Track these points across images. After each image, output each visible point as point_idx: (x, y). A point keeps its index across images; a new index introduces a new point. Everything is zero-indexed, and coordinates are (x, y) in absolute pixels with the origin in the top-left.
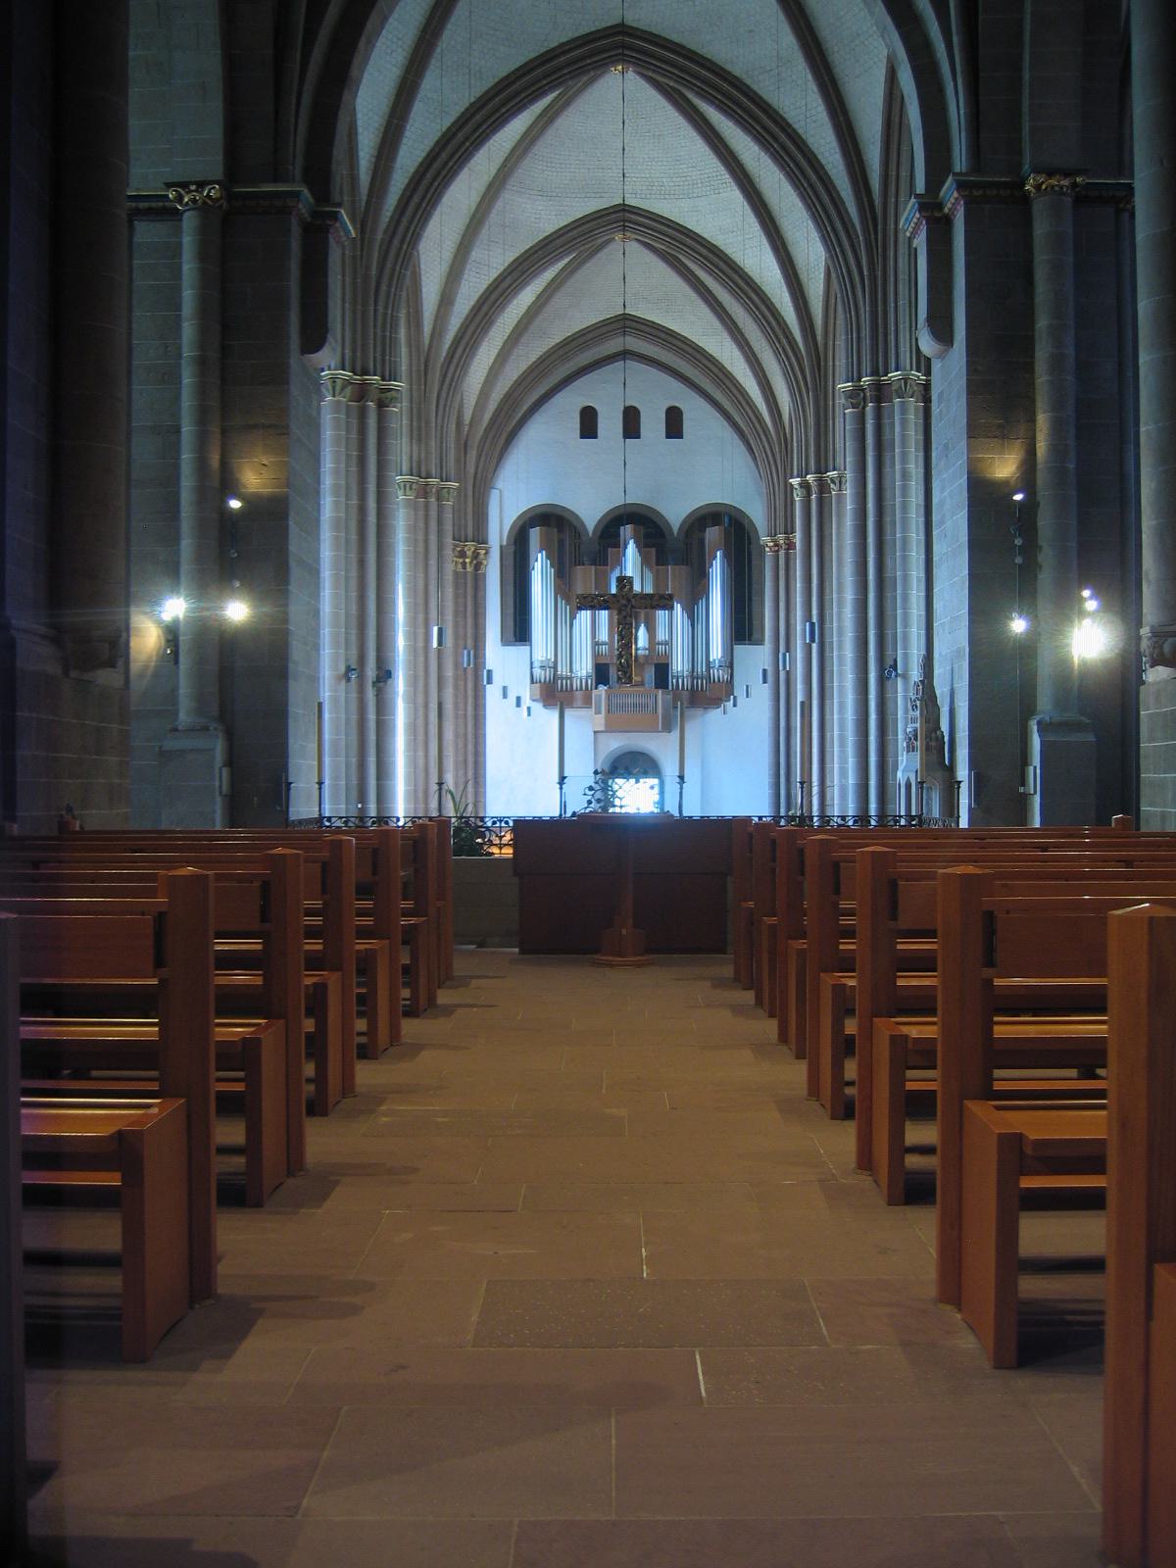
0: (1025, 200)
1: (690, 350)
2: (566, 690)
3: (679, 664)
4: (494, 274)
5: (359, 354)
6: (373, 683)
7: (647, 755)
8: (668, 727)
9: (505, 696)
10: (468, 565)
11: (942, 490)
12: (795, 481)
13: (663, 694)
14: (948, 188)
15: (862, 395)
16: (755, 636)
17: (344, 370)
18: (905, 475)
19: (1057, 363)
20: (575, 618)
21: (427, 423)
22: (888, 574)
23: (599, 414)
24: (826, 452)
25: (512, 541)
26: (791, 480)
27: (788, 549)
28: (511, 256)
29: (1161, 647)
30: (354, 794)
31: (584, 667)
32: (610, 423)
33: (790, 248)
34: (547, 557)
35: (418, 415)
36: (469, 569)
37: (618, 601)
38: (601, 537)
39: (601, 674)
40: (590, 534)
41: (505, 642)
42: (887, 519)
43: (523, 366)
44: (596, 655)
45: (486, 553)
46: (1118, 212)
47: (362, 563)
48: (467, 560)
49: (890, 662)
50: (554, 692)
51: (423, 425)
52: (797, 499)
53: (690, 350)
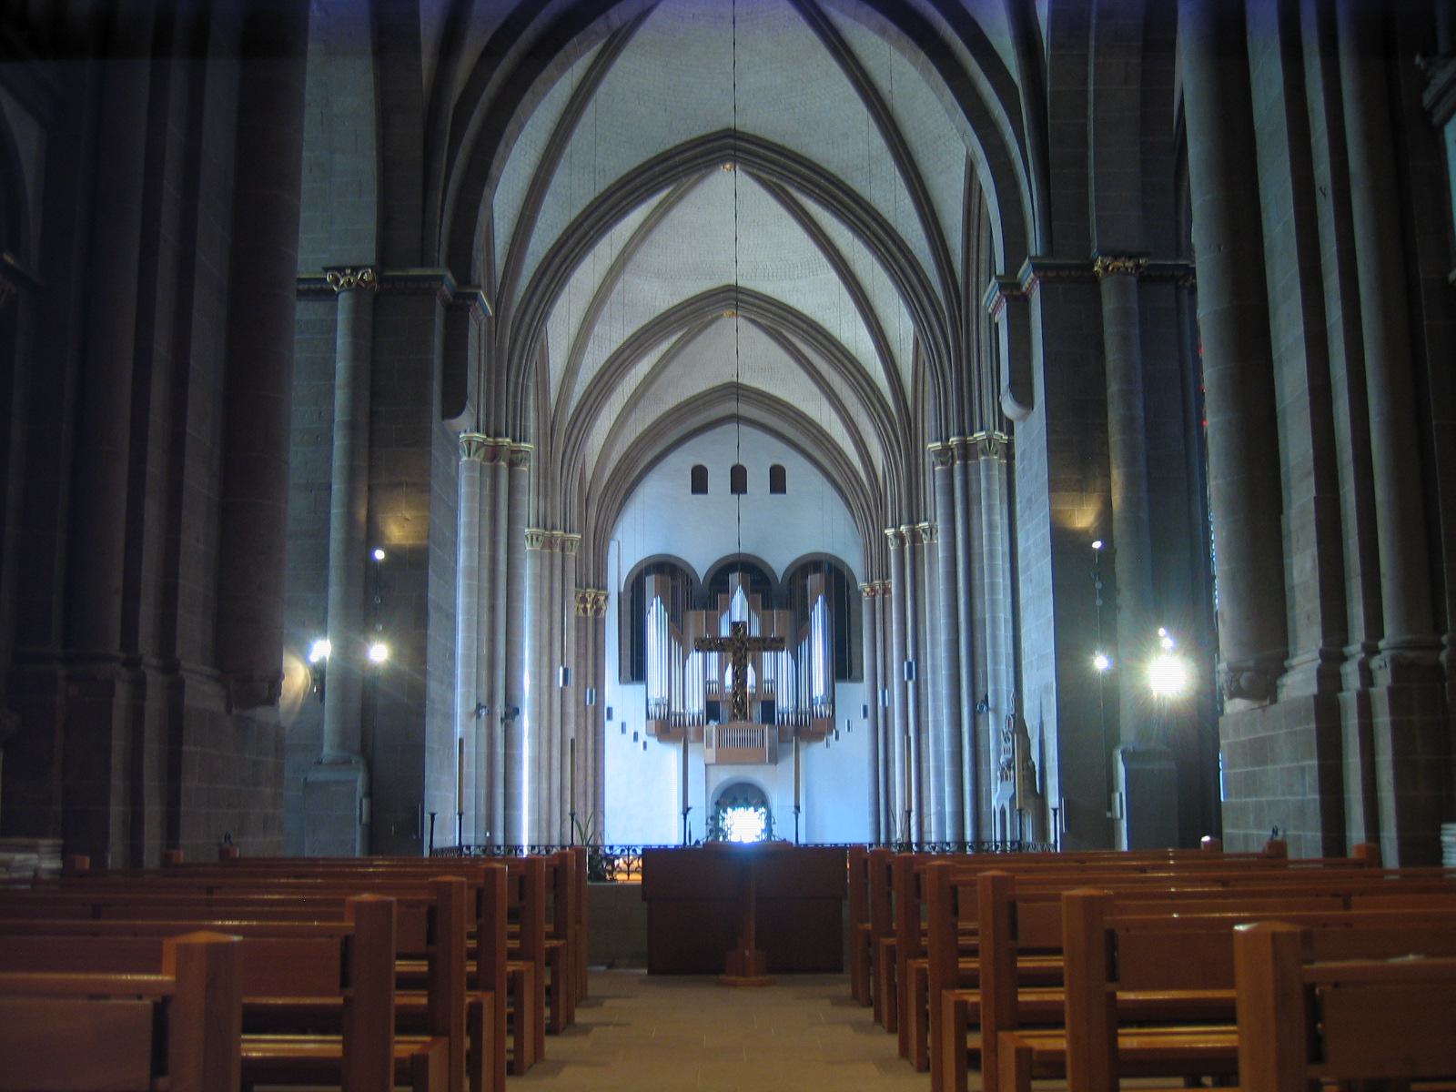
0: (1095, 280)
1: (791, 414)
3: (784, 702)
4: (615, 347)
5: (492, 418)
6: (501, 719)
8: (774, 759)
9: (623, 730)
11: (1027, 539)
12: (890, 532)
14: (1025, 271)
15: (950, 454)
16: (855, 673)
17: (478, 431)
18: (991, 526)
19: (1128, 423)
21: (553, 479)
22: (978, 616)
24: (918, 505)
25: (630, 588)
26: (886, 531)
27: (883, 595)
28: (630, 330)
29: (1238, 681)
30: (483, 824)
31: (696, 705)
32: (719, 481)
33: (882, 324)
35: (545, 476)
36: (590, 613)
37: (734, 644)
38: (711, 584)
39: (712, 710)
40: (701, 580)
42: (976, 566)
43: (640, 429)
44: (707, 693)
45: (607, 598)
46: (1178, 289)
47: (493, 609)
48: (589, 606)
49: (981, 697)
50: (668, 727)
51: (549, 483)
52: (892, 548)
53: (791, 414)
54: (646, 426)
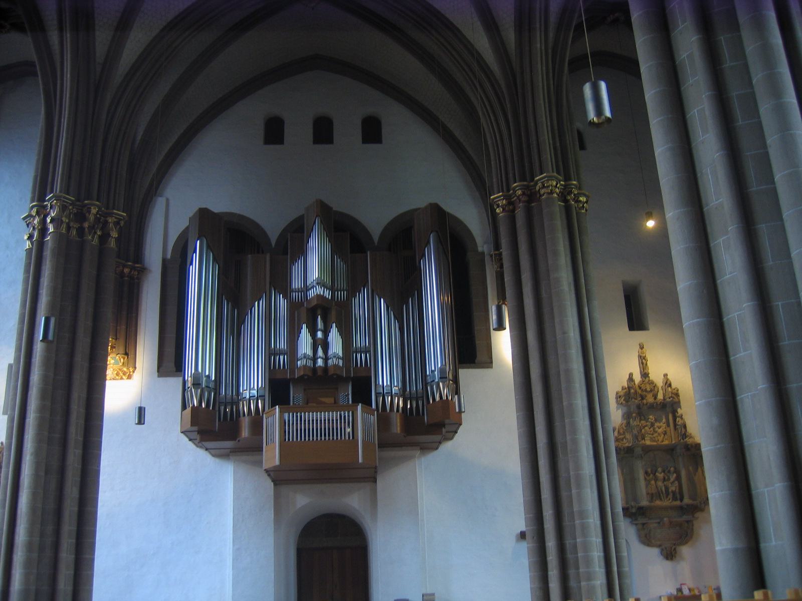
7: (348, 517)
16: (480, 357)
27: (529, 202)
48: (86, 225)
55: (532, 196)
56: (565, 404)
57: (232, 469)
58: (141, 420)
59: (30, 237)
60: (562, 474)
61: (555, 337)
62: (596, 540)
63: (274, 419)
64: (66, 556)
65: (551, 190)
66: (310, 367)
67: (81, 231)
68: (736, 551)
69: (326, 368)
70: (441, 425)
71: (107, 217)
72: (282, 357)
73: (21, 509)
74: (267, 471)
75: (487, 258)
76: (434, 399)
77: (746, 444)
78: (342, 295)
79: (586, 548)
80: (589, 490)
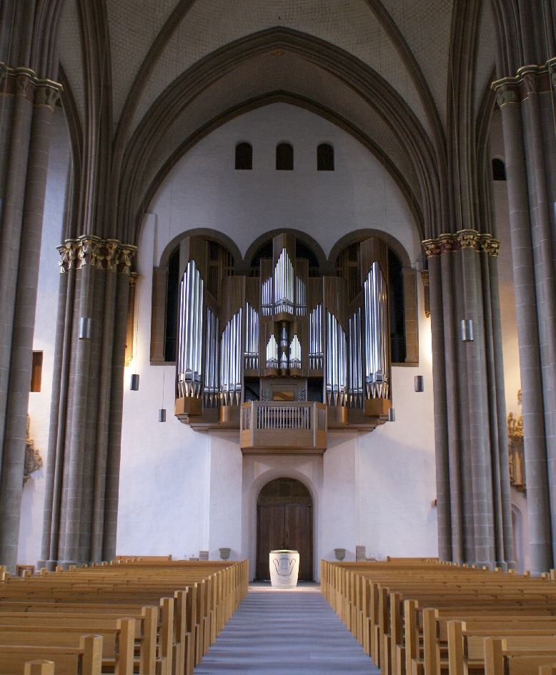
2: (214, 406)
3: (336, 378)
7: (301, 483)
10: (109, 263)
13: (318, 408)
16: (409, 357)
20: (224, 329)
23: (253, 148)
27: (451, 249)
31: (232, 378)
32: (264, 157)
34: (197, 268)
36: (112, 268)
39: (251, 384)
41: (154, 360)
54: (184, 70)
55: (454, 245)
56: (471, 411)
57: (210, 445)
58: (163, 419)
59: (65, 264)
60: (466, 464)
61: (466, 358)
62: (488, 515)
63: (250, 409)
64: (99, 510)
65: (469, 243)
66: (276, 369)
67: (105, 263)
68: (539, 545)
69: (288, 371)
70: (378, 417)
71: (122, 250)
72: (254, 360)
73: (68, 475)
74: (242, 449)
75: (419, 275)
76: (371, 395)
77: (550, 486)
78: (300, 311)
79: (481, 520)
80: (485, 478)
